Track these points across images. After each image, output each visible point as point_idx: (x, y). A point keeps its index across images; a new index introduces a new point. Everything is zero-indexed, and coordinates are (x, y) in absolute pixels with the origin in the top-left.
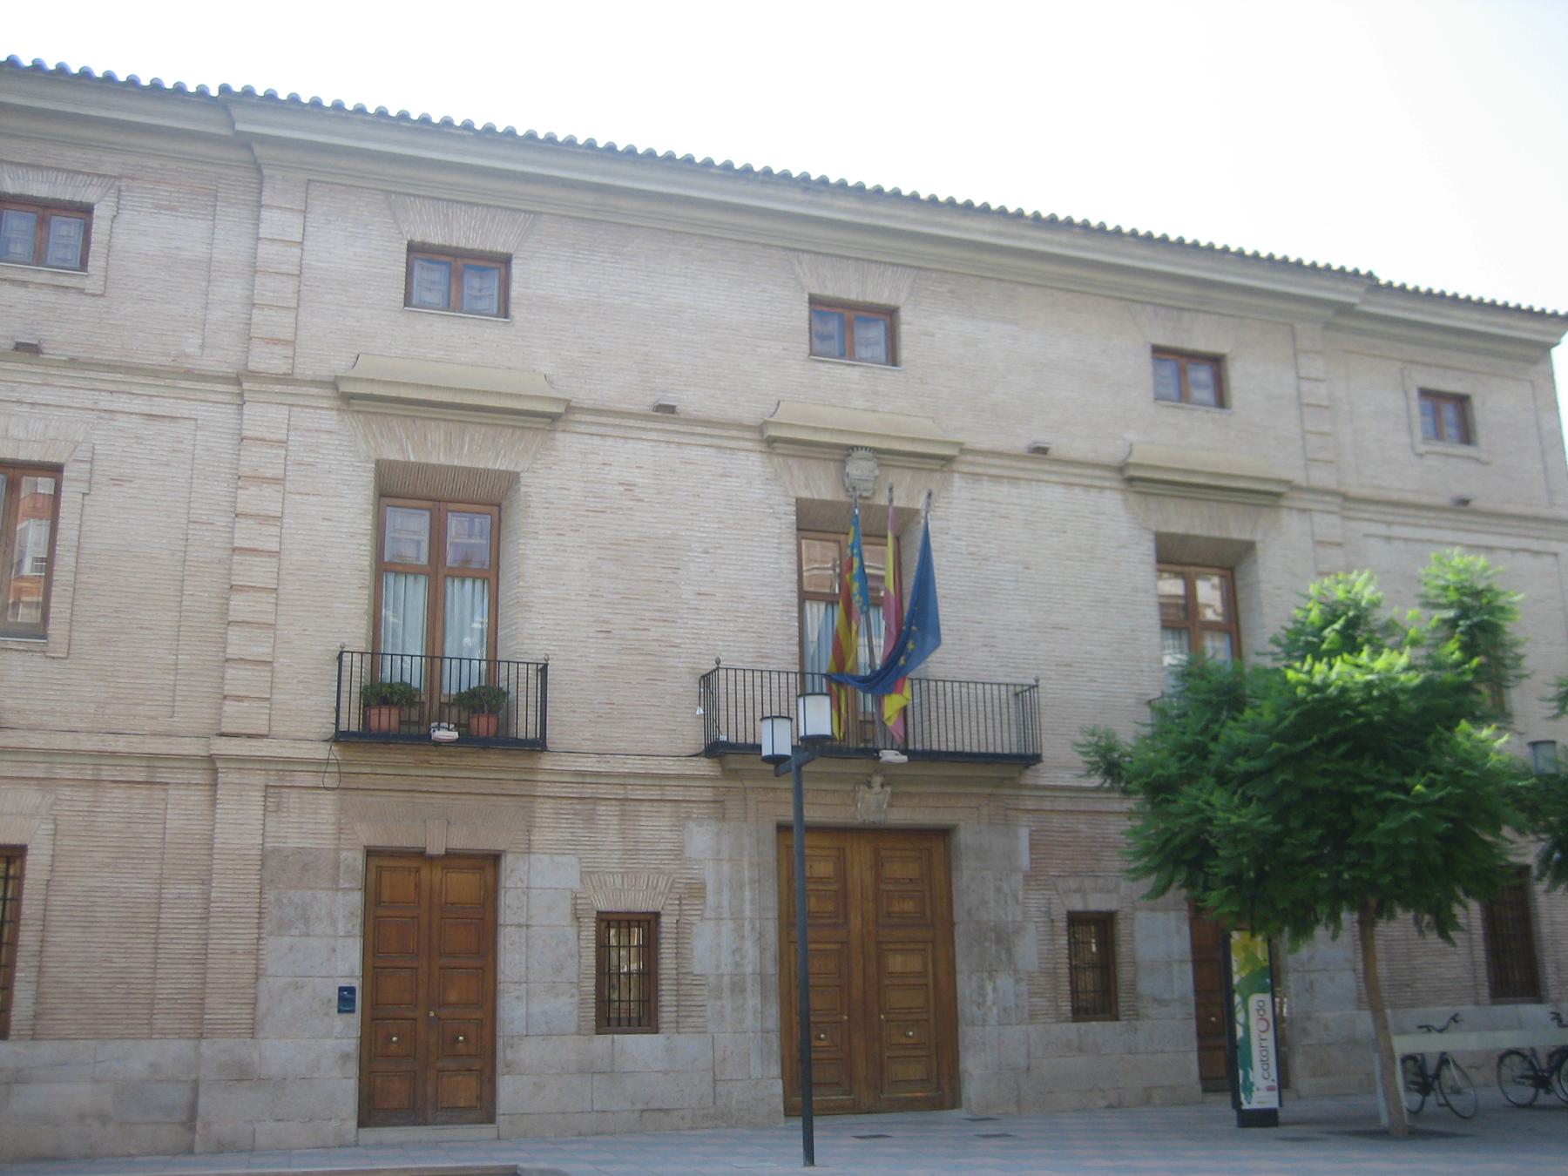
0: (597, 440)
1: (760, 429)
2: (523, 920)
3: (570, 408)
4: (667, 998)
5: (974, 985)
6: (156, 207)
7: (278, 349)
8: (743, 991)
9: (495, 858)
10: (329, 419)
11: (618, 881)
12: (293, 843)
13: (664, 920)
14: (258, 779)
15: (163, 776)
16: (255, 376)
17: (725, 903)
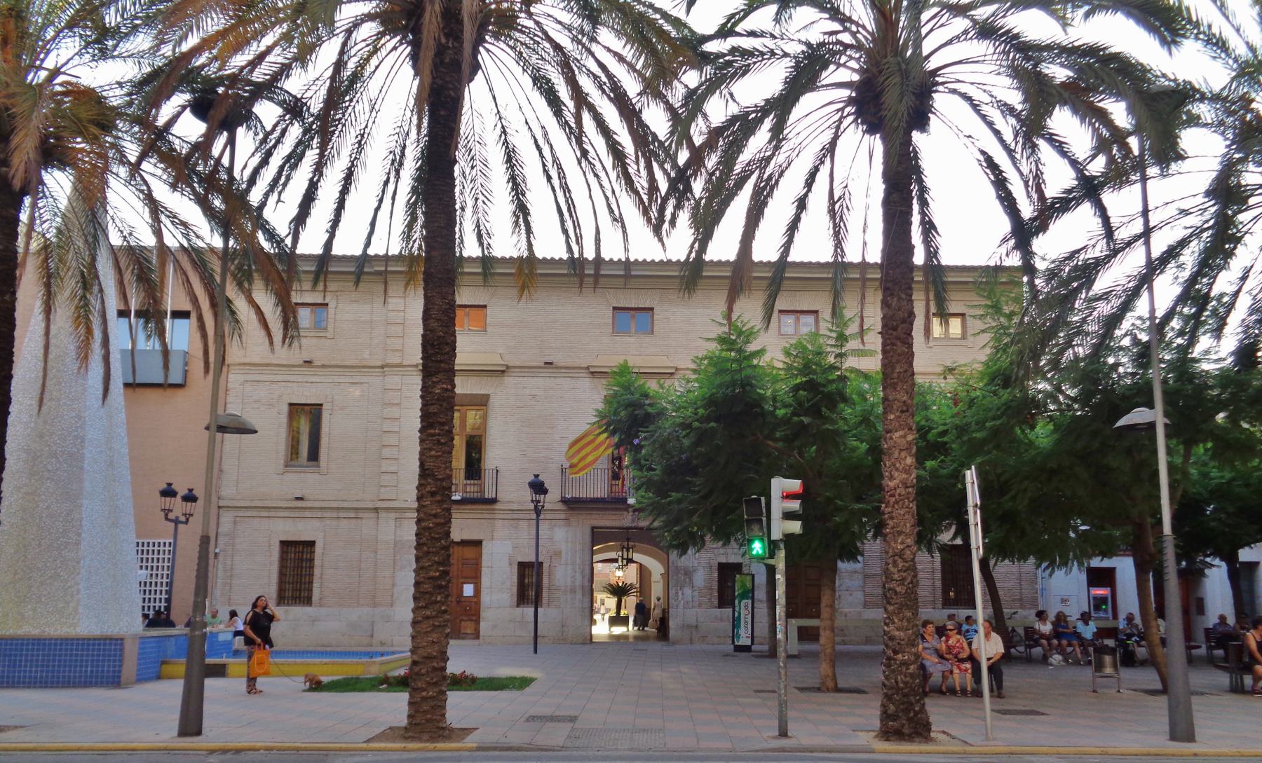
1: (588, 368)
3: (508, 367)
7: (397, 354)
9: (478, 543)
14: (393, 515)
15: (360, 515)
16: (388, 365)
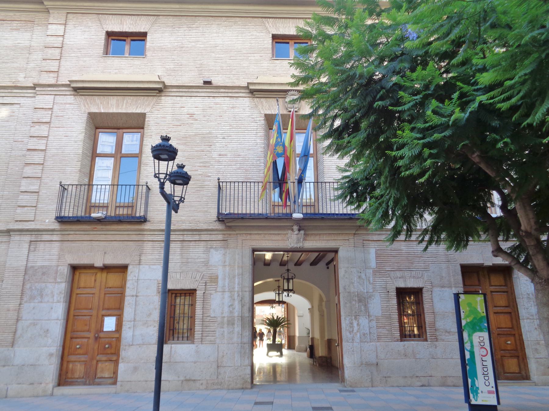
0: (179, 98)
1: (247, 88)
2: (135, 294)
3: (166, 87)
4: (198, 328)
5: (347, 322)
6: (11, 29)
7: (52, 75)
8: (233, 324)
9: (123, 269)
10: (71, 99)
11: (178, 276)
12: (39, 264)
13: (197, 292)
14: (27, 238)
17: (227, 285)
